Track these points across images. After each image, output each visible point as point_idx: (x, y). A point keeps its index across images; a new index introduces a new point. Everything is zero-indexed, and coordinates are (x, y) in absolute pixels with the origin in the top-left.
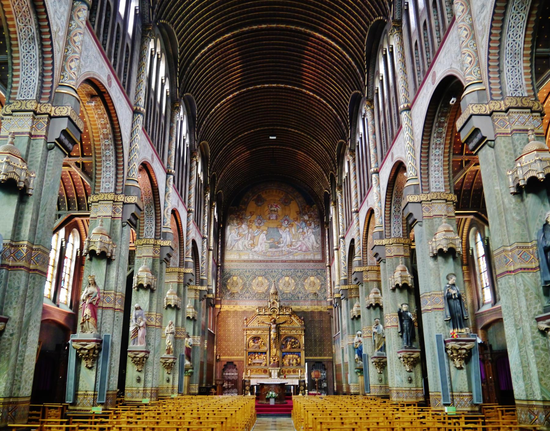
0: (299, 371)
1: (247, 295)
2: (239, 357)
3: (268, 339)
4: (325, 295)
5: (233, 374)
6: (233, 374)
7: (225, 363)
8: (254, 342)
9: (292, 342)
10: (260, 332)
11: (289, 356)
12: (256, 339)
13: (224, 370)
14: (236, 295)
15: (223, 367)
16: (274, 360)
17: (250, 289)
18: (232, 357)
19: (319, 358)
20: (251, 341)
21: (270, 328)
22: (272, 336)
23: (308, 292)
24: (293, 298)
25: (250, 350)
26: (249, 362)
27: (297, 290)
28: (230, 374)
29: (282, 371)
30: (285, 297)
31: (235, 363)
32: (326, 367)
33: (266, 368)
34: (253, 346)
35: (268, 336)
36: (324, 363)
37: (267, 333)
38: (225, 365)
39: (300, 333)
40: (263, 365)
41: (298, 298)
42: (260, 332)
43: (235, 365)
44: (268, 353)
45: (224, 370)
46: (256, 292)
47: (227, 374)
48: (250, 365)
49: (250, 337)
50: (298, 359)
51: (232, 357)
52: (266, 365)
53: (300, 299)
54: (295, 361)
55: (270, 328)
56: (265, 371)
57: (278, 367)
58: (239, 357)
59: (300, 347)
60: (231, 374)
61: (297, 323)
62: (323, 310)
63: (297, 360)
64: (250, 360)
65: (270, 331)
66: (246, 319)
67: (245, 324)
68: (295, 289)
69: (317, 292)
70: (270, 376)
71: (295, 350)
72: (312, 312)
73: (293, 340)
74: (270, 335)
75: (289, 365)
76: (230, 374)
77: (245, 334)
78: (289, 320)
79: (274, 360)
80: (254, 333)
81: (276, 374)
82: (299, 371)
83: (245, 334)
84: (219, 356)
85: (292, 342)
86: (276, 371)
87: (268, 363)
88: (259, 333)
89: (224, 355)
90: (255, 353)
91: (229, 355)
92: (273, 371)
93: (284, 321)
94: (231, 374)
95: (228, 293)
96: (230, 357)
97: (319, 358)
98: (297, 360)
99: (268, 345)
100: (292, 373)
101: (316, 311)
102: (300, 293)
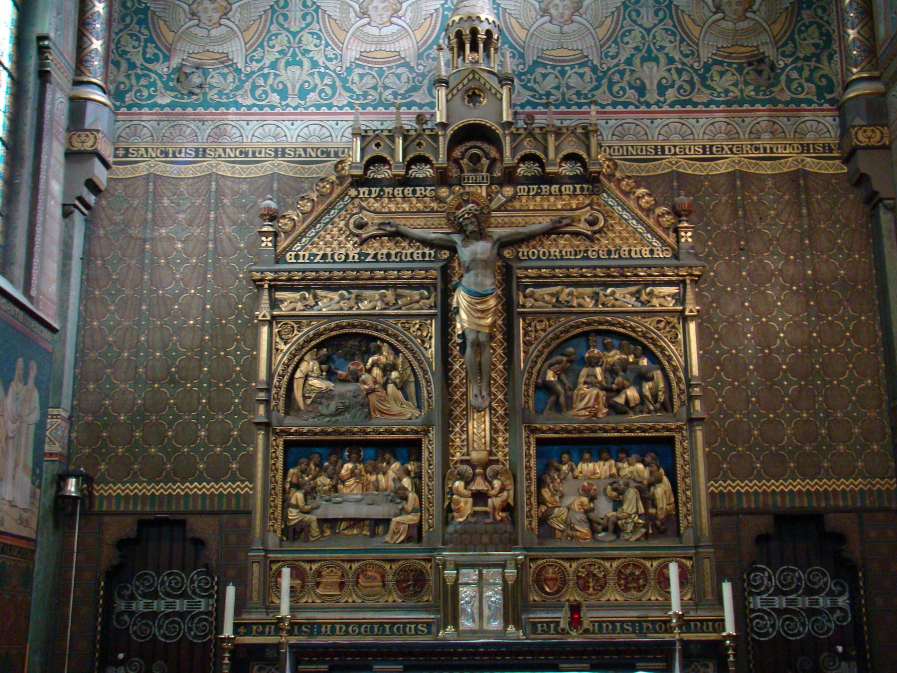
0: (673, 571)
1: (293, 76)
2: (227, 488)
3: (432, 351)
4: (825, 69)
5: (180, 605)
6: (180, 605)
7: (128, 527)
8: (330, 375)
9: (611, 371)
10: (369, 303)
11: (586, 467)
12: (341, 346)
13: (117, 576)
14: (215, 80)
15: (108, 556)
16: (480, 497)
17: (308, 40)
18: (178, 489)
19: (798, 485)
20: (309, 365)
21: (446, 272)
22: (463, 321)
23: (705, 54)
24: (602, 95)
25: (300, 425)
26: (294, 515)
27: (634, 39)
28: (159, 605)
29: (540, 580)
30: (550, 83)
31: (200, 526)
32: (854, 550)
33: (415, 555)
34: (324, 396)
35: (433, 328)
36: (834, 522)
37: (422, 303)
38: (121, 544)
39: (670, 305)
40: (393, 538)
41: (641, 90)
42: (369, 303)
43: (199, 543)
44: (431, 446)
45: (117, 576)
46: (352, 54)
47: (140, 605)
48: (295, 533)
49: (298, 336)
50: (661, 491)
51: (178, 489)
52: (416, 534)
53: (652, 96)
54: (632, 504)
55: (446, 272)
56: (412, 582)
57: (510, 543)
58: (227, 488)
59: (667, 407)
60: (156, 605)
61: (633, 232)
62: (811, 164)
63: (648, 500)
64: (298, 496)
65: (447, 293)
66: (273, 217)
67: (267, 242)
68: (616, 37)
69: (770, 52)
70: (449, 608)
71: (637, 423)
72: (739, 180)
73: (615, 356)
74: (447, 316)
75: (594, 531)
76: (159, 605)
77: (264, 311)
78: (585, 214)
79: (480, 497)
80: (329, 303)
81: (493, 595)
82: (673, 571)
83: (264, 311)
84: (86, 480)
85: (611, 371)
86: (492, 575)
87: (433, 520)
88: (365, 306)
89: (124, 473)
90: (336, 447)
91: (155, 475)
92: (472, 575)
93: (543, 222)
94: (156, 605)
95: (162, 68)
96: (160, 489)
97: (798, 485)
98: (648, 500)
99: (432, 390)
100: (613, 595)
101: (766, 169)
102: (649, 58)
